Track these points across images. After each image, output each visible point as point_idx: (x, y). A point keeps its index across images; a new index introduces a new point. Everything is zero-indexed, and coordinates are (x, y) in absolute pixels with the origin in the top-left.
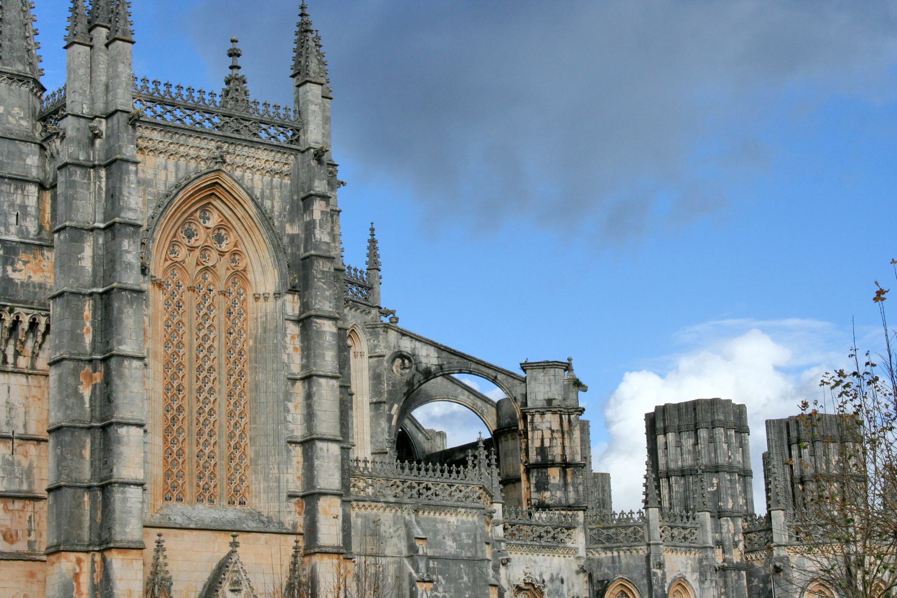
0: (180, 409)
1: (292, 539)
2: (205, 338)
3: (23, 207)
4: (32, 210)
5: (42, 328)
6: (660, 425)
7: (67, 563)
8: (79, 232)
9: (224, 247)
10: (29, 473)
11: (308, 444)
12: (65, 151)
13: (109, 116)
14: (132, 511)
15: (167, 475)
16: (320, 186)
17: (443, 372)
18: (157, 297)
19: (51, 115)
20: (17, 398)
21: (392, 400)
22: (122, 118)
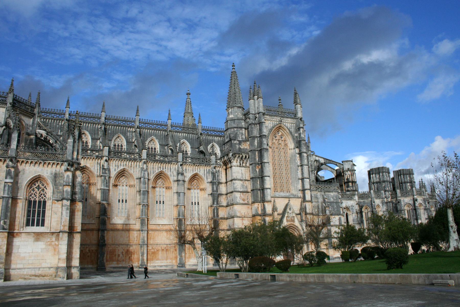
0: (276, 173)
1: (300, 199)
2: (280, 158)
3: (242, 133)
4: (244, 134)
5: (247, 157)
6: (371, 173)
7: (256, 205)
8: (254, 137)
9: (283, 139)
10: (246, 187)
11: (302, 179)
12: (250, 121)
13: (258, 114)
14: (269, 194)
15: (274, 187)
16: (301, 125)
17: (325, 164)
18: (270, 150)
19: (246, 115)
20: (243, 172)
21: (315, 170)
22: (261, 114)
